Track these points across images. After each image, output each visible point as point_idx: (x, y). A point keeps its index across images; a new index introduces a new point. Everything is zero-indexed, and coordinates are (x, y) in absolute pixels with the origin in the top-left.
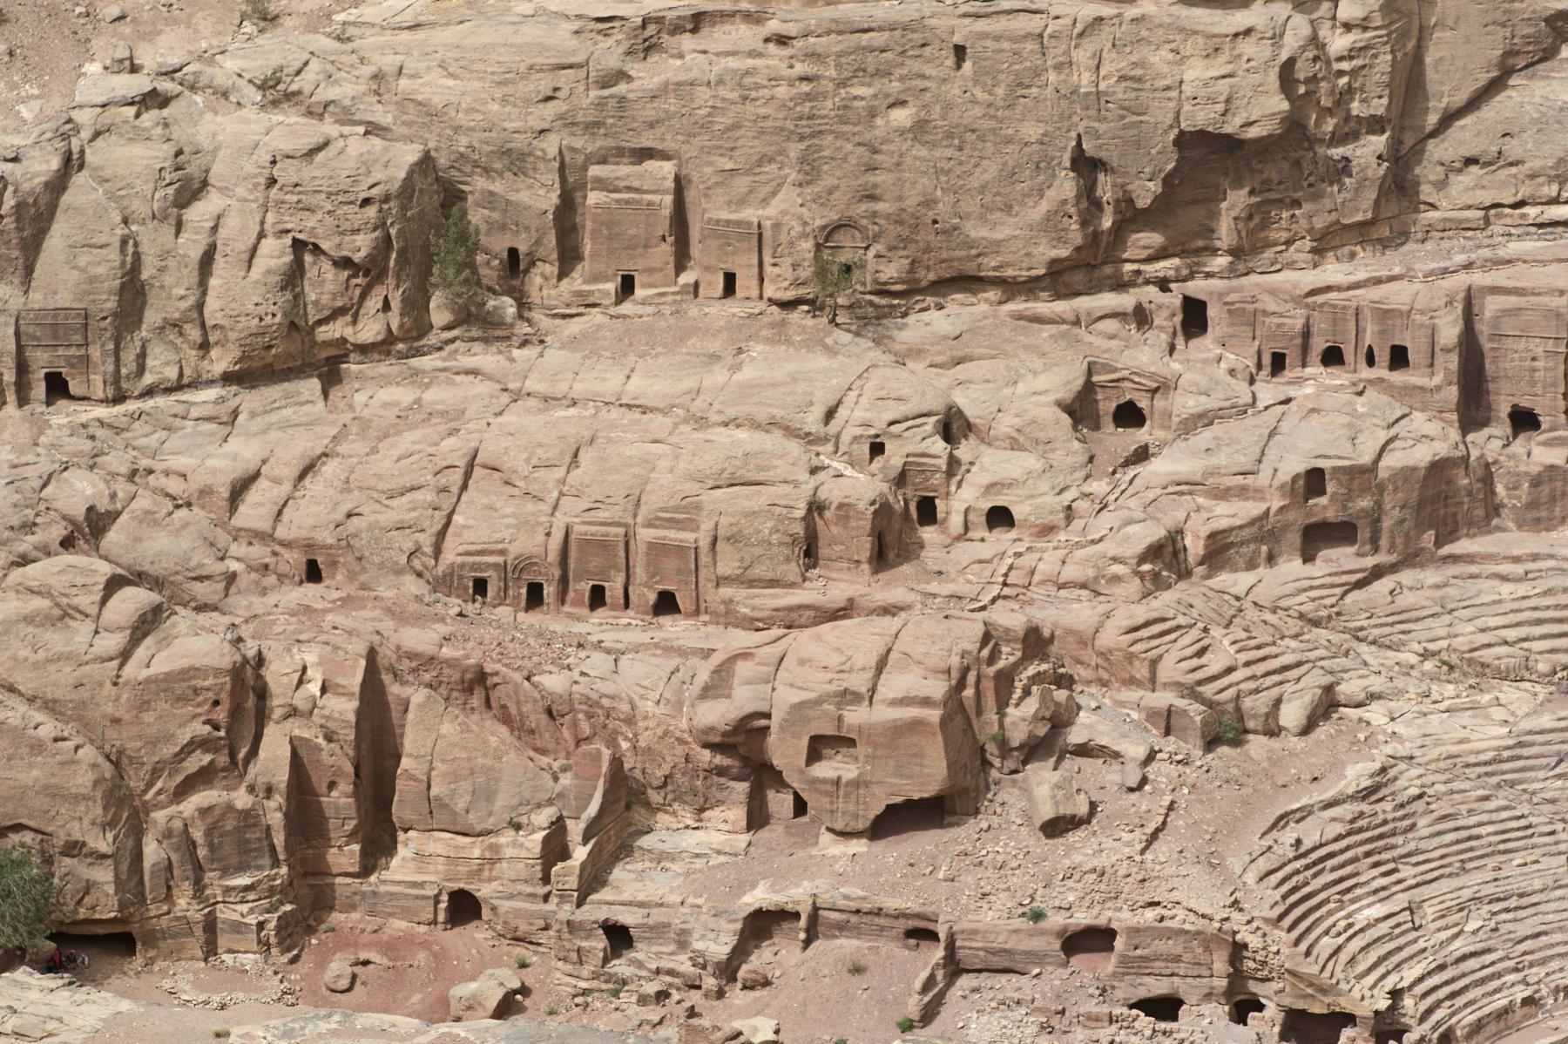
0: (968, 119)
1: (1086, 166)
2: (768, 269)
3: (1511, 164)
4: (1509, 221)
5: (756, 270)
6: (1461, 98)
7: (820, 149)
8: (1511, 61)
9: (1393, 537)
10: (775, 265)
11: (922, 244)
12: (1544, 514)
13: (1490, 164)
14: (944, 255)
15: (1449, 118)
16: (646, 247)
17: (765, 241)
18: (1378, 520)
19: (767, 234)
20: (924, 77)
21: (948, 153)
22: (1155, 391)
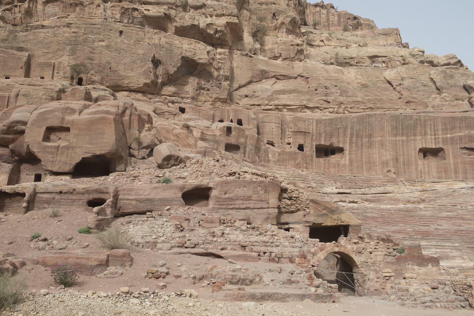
0: (122, 47)
1: (156, 63)
2: (55, 74)
3: (256, 97)
4: (257, 109)
5: (51, 75)
6: (243, 83)
7: (77, 48)
8: (253, 79)
9: (249, 154)
10: (58, 73)
11: (106, 74)
12: (281, 164)
13: (251, 97)
14: (112, 78)
15: (240, 87)
16: (15, 69)
17: (55, 67)
18: (245, 147)
19: (56, 66)
20: (110, 36)
21: (116, 54)
22: (175, 115)
